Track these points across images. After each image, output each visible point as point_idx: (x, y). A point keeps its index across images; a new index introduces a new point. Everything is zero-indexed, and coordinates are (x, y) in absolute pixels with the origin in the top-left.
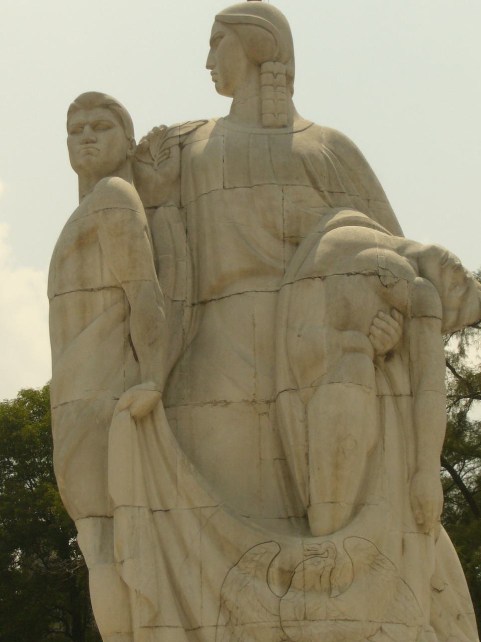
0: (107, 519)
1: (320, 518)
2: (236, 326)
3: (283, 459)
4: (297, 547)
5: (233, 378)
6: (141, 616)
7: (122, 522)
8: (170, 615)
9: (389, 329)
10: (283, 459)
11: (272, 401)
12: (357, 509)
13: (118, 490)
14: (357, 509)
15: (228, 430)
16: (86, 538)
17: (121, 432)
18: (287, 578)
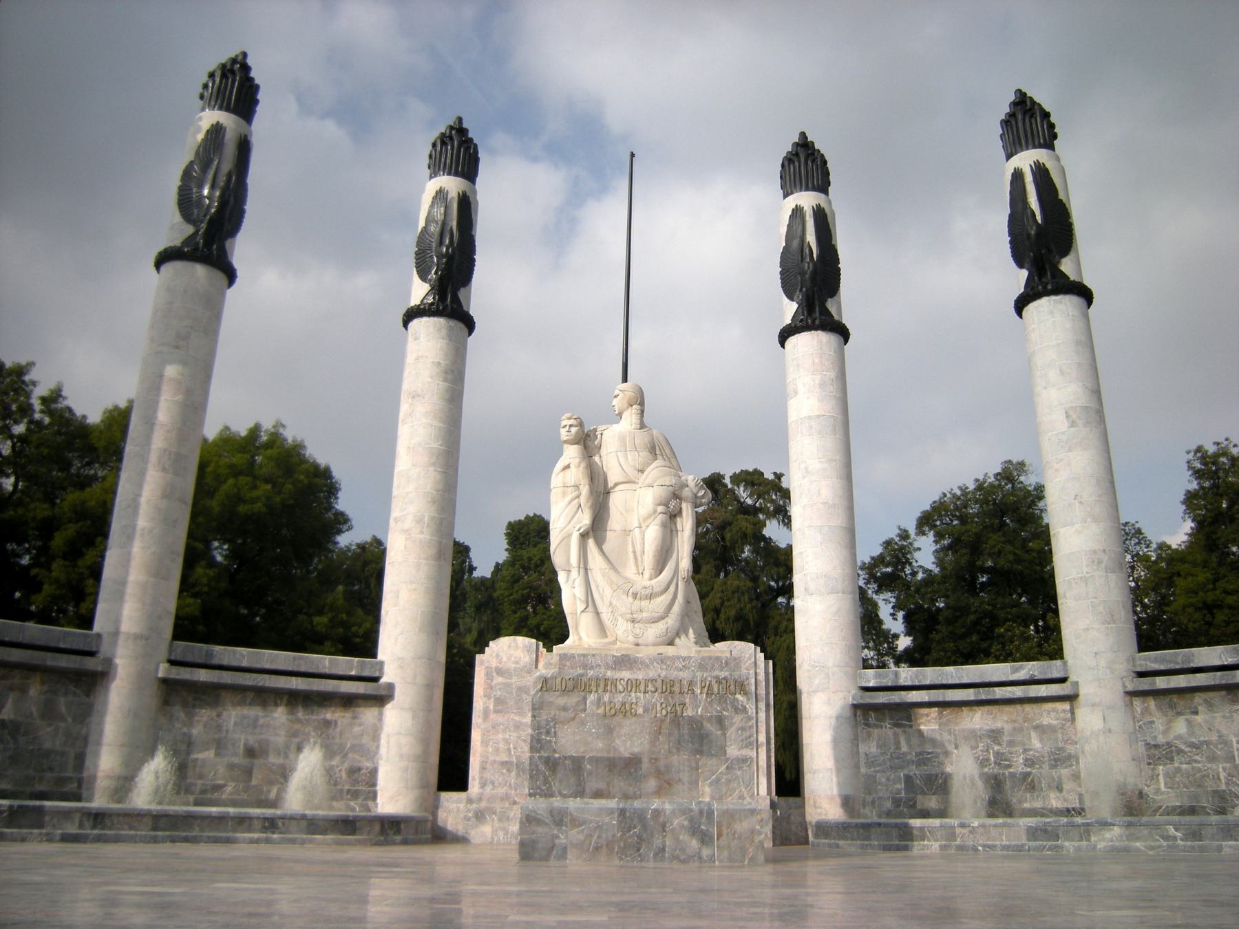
8: (591, 608)
16: (561, 578)
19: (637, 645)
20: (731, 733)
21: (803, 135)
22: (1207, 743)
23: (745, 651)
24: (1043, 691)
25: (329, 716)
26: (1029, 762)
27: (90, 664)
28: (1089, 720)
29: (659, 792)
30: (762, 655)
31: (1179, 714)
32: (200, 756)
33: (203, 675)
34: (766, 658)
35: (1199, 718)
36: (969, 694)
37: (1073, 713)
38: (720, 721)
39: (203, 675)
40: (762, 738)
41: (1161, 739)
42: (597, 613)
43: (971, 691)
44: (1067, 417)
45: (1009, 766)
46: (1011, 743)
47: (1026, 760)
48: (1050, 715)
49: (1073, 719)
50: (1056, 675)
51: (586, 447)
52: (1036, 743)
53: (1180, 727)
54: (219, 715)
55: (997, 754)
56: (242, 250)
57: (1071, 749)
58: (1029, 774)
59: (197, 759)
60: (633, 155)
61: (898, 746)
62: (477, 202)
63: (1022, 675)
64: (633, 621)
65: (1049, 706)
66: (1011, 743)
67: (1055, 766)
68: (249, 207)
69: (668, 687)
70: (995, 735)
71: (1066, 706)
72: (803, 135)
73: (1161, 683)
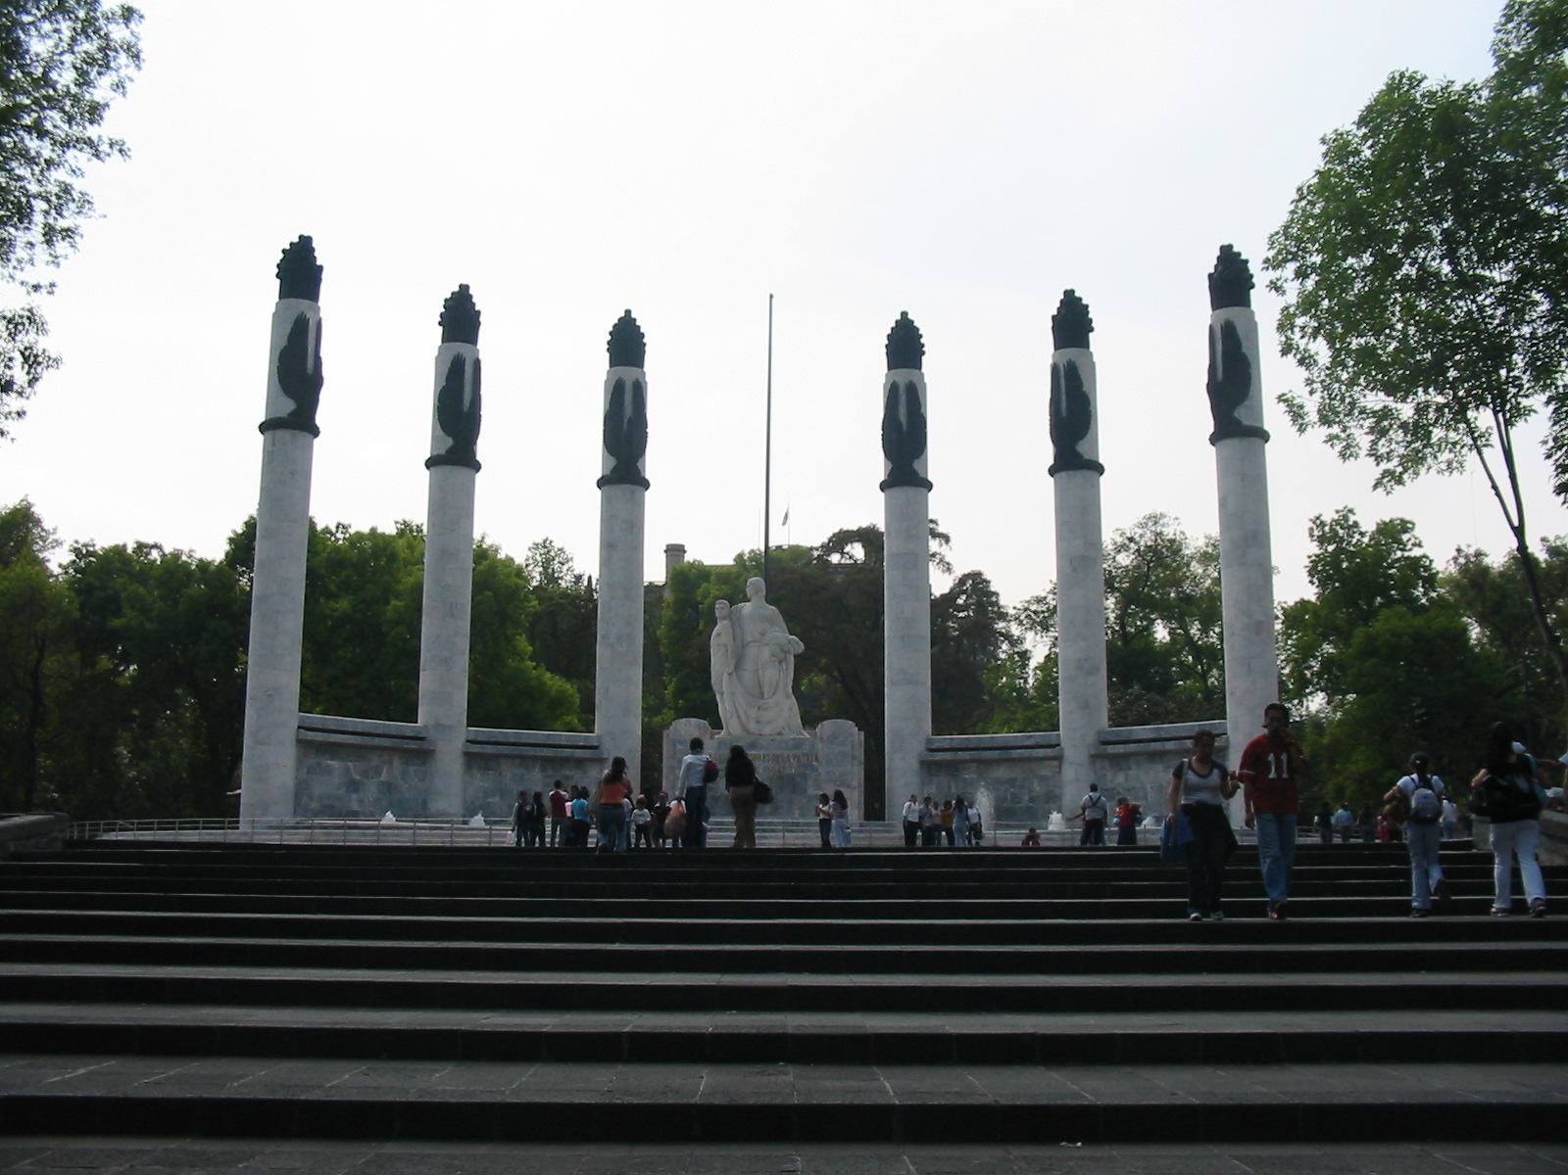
0: (722, 694)
1: (766, 696)
2: (751, 652)
3: (759, 682)
4: (761, 702)
5: (749, 665)
6: (729, 715)
7: (725, 695)
9: (782, 656)
10: (759, 682)
11: (757, 670)
12: (774, 694)
13: (724, 689)
14: (774, 694)
15: (747, 675)
16: (718, 697)
17: (726, 674)
18: (759, 708)
19: (761, 735)
20: (810, 783)
21: (904, 314)
22: (1133, 788)
23: (849, 726)
24: (1041, 752)
25: (568, 773)
26: (1032, 800)
27: (425, 746)
28: (1069, 772)
29: (771, 814)
30: (856, 729)
31: (1121, 769)
32: (490, 800)
33: (490, 749)
34: (859, 730)
35: (1130, 772)
36: (995, 754)
37: (1060, 767)
38: (804, 776)
39: (490, 749)
40: (855, 783)
41: (1110, 785)
42: (739, 717)
43: (997, 752)
44: (1071, 563)
45: (1019, 802)
46: (1021, 787)
47: (1030, 799)
48: (1045, 770)
49: (1060, 772)
50: (1055, 742)
51: (731, 619)
52: (1037, 788)
53: (1121, 778)
54: (500, 774)
55: (1012, 794)
56: (483, 449)
57: (1057, 791)
58: (1032, 807)
59: (489, 803)
60: (771, 296)
61: (949, 788)
62: (646, 383)
63: (1031, 742)
64: (758, 722)
65: (1048, 763)
66: (1021, 787)
67: (1048, 803)
68: (484, 412)
69: (776, 758)
70: (1012, 782)
71: (1056, 763)
72: (904, 314)
73: (1111, 749)
